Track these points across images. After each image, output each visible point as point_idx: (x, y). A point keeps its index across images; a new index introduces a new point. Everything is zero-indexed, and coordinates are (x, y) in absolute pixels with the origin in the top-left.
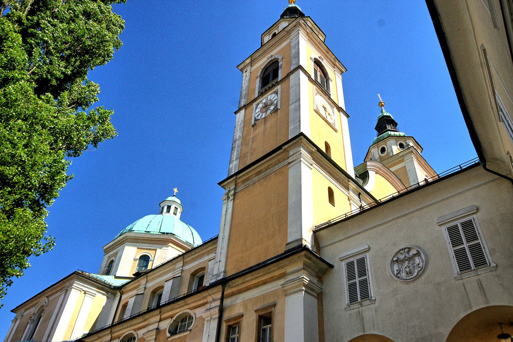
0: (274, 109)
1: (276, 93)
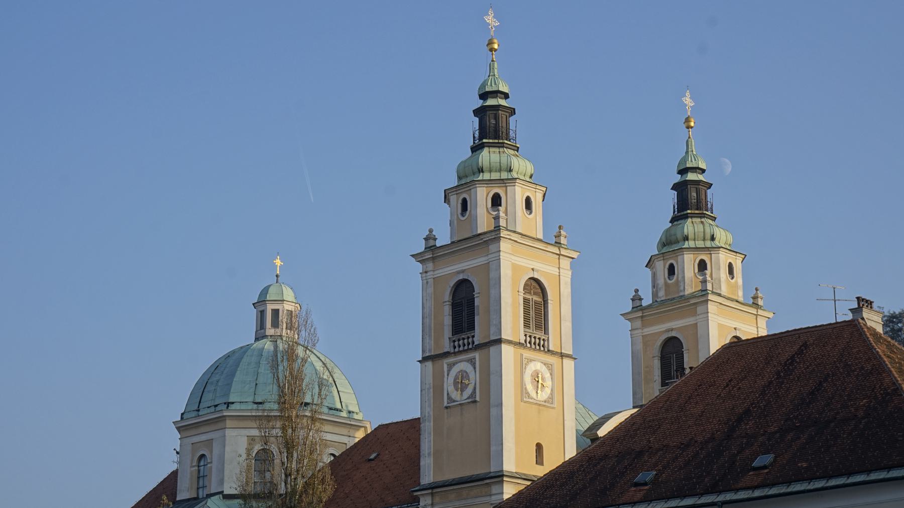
1: (472, 362)
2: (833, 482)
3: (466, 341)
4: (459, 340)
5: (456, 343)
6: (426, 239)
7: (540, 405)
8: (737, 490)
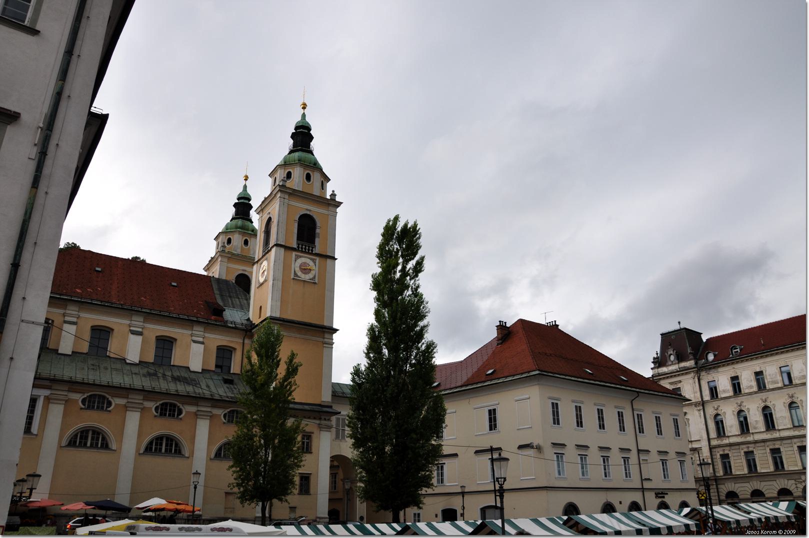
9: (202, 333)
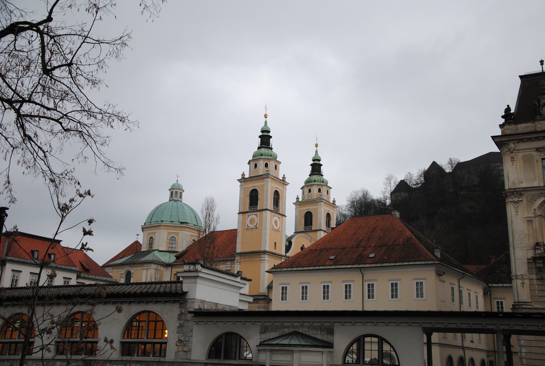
0: (256, 225)
1: (256, 215)
2: (397, 264)
3: (254, 208)
4: (252, 208)
5: (251, 209)
6: (242, 175)
7: (276, 230)
8: (365, 264)
9: (230, 265)
